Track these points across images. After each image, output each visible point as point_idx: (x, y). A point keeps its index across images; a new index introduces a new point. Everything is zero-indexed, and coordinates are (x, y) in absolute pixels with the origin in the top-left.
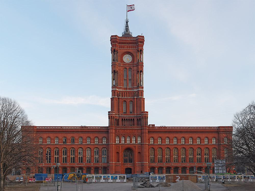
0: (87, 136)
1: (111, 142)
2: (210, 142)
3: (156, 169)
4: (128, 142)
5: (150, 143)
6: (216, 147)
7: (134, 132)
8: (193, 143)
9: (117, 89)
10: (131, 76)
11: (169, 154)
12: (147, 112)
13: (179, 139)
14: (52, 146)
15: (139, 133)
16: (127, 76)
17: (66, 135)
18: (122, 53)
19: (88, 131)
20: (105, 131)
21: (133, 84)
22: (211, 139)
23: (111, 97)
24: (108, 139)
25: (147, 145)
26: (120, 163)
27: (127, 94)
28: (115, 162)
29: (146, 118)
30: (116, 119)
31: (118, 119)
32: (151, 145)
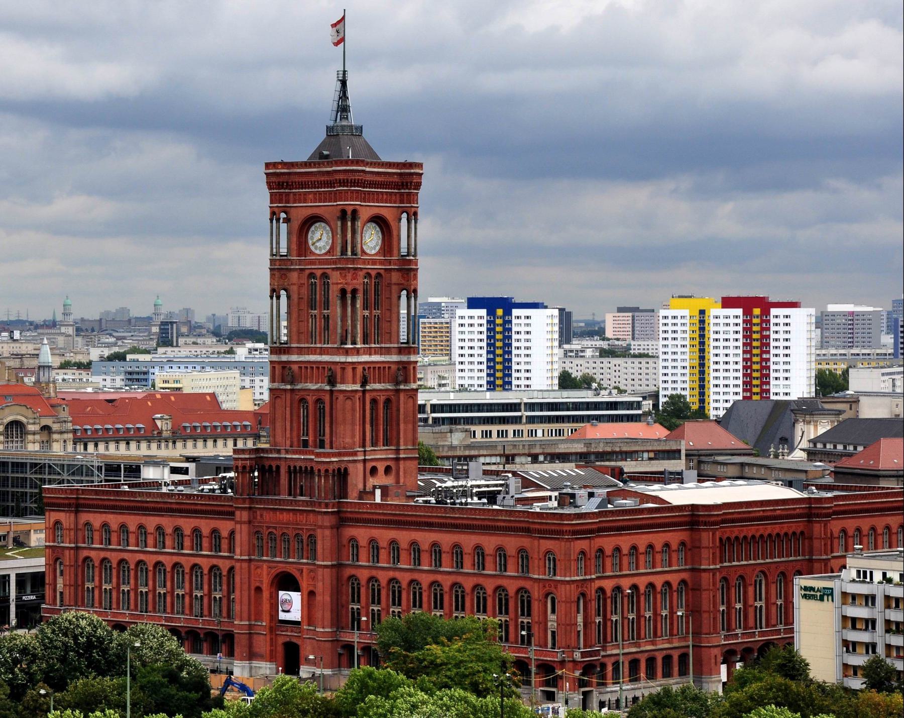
7: (298, 519)
17: (144, 520)
26: (264, 624)
28: (249, 620)
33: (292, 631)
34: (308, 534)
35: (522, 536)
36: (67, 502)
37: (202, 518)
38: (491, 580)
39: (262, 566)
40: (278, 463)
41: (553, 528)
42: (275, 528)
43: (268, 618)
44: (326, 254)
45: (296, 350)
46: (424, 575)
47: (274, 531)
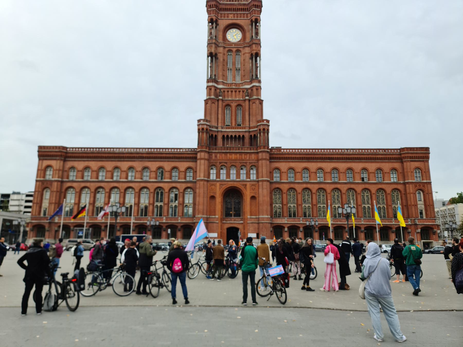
0: (158, 166)
1: (201, 176)
2: (386, 178)
3: (286, 229)
4: (233, 177)
5: (273, 180)
6: (399, 187)
7: (243, 158)
8: (354, 180)
9: (216, 85)
10: (239, 64)
11: (310, 199)
12: (268, 121)
13: (327, 171)
14: (92, 184)
15: (253, 160)
16: (234, 64)
17: (119, 164)
18: (224, 26)
19: (161, 155)
20: (191, 156)
21: (243, 77)
22: (388, 171)
23: (205, 99)
24: (196, 172)
25: (268, 183)
26: (217, 217)
27: (232, 94)
28: (207, 215)
29: (266, 131)
30: (212, 135)
31: (216, 136)
32: (276, 183)
33: (234, 220)
34: (250, 165)
35: (393, 162)
36: (59, 154)
37: (165, 161)
38: (374, 186)
39: (216, 184)
40: (217, 134)
41: (421, 155)
42: (226, 163)
43: (220, 213)
44: (238, 42)
45: (222, 83)
46: (328, 185)
47: (225, 164)
